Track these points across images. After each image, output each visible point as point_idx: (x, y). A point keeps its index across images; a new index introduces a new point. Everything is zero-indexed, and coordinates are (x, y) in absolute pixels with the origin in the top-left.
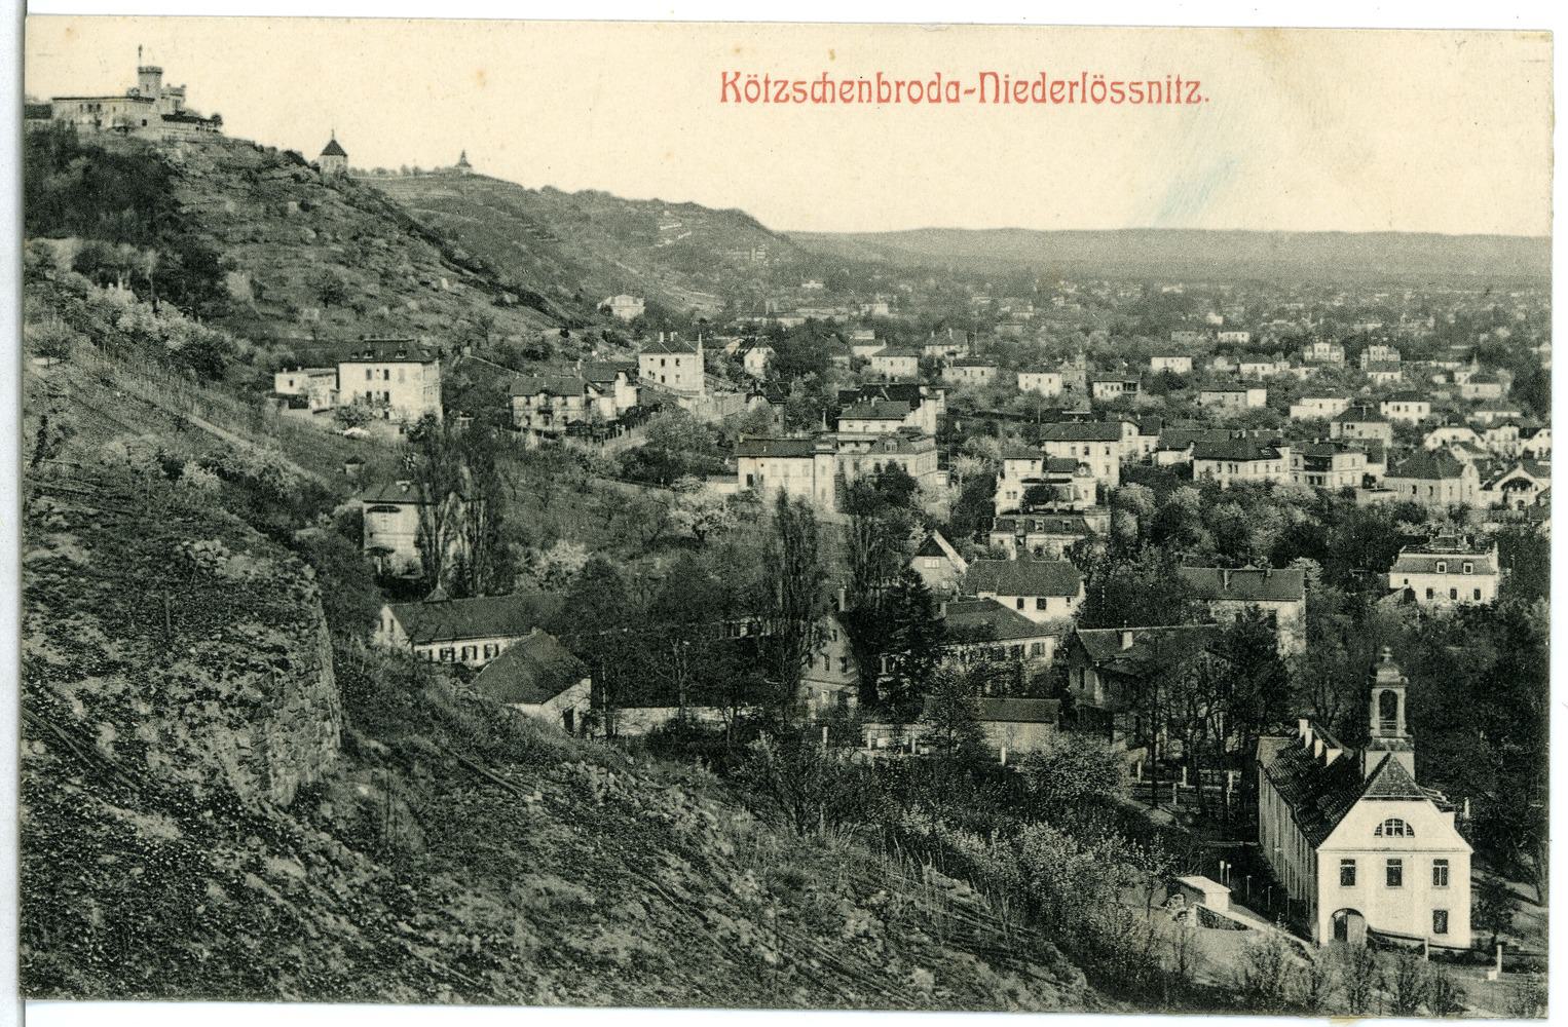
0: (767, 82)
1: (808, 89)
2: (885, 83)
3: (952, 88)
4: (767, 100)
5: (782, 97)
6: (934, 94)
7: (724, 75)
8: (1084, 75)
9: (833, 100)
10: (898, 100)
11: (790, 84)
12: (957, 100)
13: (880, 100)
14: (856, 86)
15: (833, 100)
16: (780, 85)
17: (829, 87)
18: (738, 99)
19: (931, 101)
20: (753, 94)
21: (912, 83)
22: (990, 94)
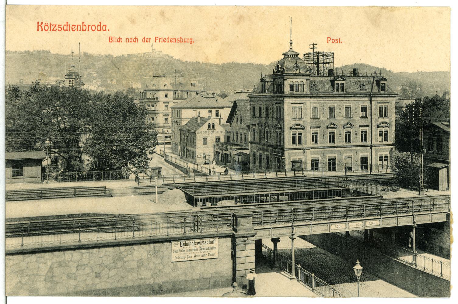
1: (62, 27)
2: (84, 25)
3: (104, 27)
4: (50, 30)
5: (55, 29)
7: (38, 23)
9: (70, 30)
11: (57, 26)
14: (76, 27)
15: (70, 30)
16: (54, 26)
17: (68, 26)
18: (42, 30)
19: (98, 30)
20: (46, 29)
21: (93, 25)
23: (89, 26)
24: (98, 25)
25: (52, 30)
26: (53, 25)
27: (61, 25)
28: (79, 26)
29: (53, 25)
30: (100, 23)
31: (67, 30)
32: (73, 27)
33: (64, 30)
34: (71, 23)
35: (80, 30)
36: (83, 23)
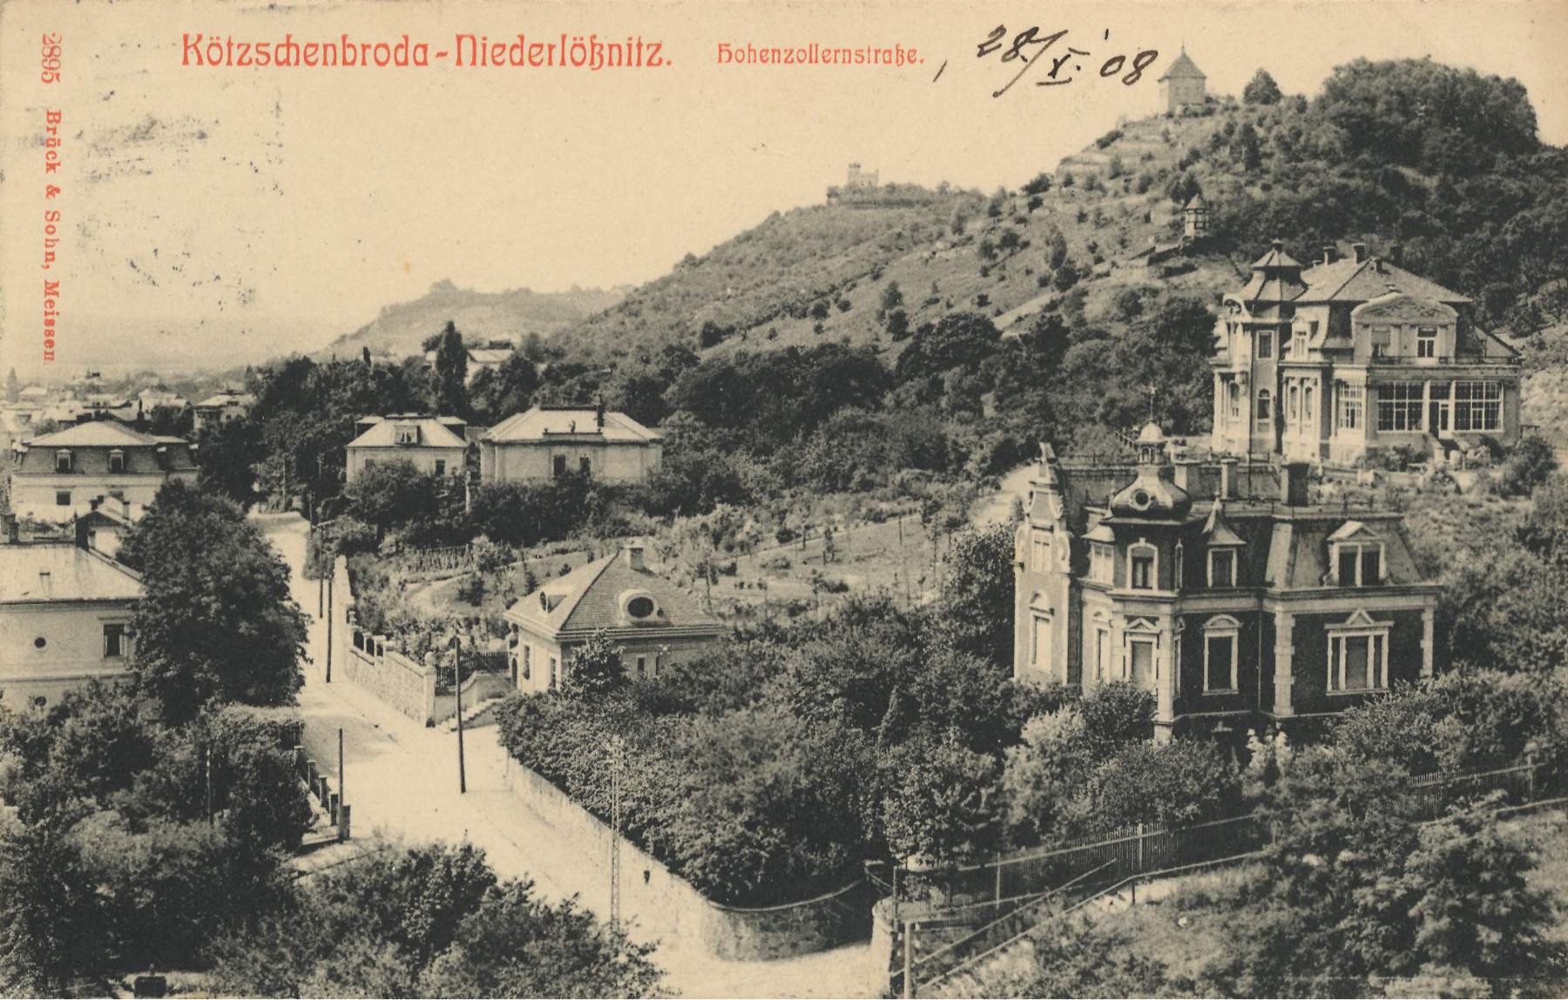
0: (230, 44)
1: (271, 50)
2: (350, 46)
3: (420, 50)
4: (229, 63)
6: (401, 58)
7: (186, 38)
8: (564, 37)
9: (297, 63)
10: (364, 63)
12: (425, 63)
13: (345, 62)
14: (321, 49)
15: (297, 63)
16: (243, 48)
17: (293, 51)
18: (200, 62)
19: (398, 64)
20: (215, 58)
21: (378, 46)
22: (467, 58)
23: (365, 47)
24: (400, 46)
25: (235, 59)
26: (239, 46)
27: (267, 45)
28: (330, 50)
29: (239, 46)
30: (522, 38)
31: (287, 62)
32: (310, 51)
33: (279, 63)
34: (301, 39)
35: (334, 63)
36: (344, 38)
